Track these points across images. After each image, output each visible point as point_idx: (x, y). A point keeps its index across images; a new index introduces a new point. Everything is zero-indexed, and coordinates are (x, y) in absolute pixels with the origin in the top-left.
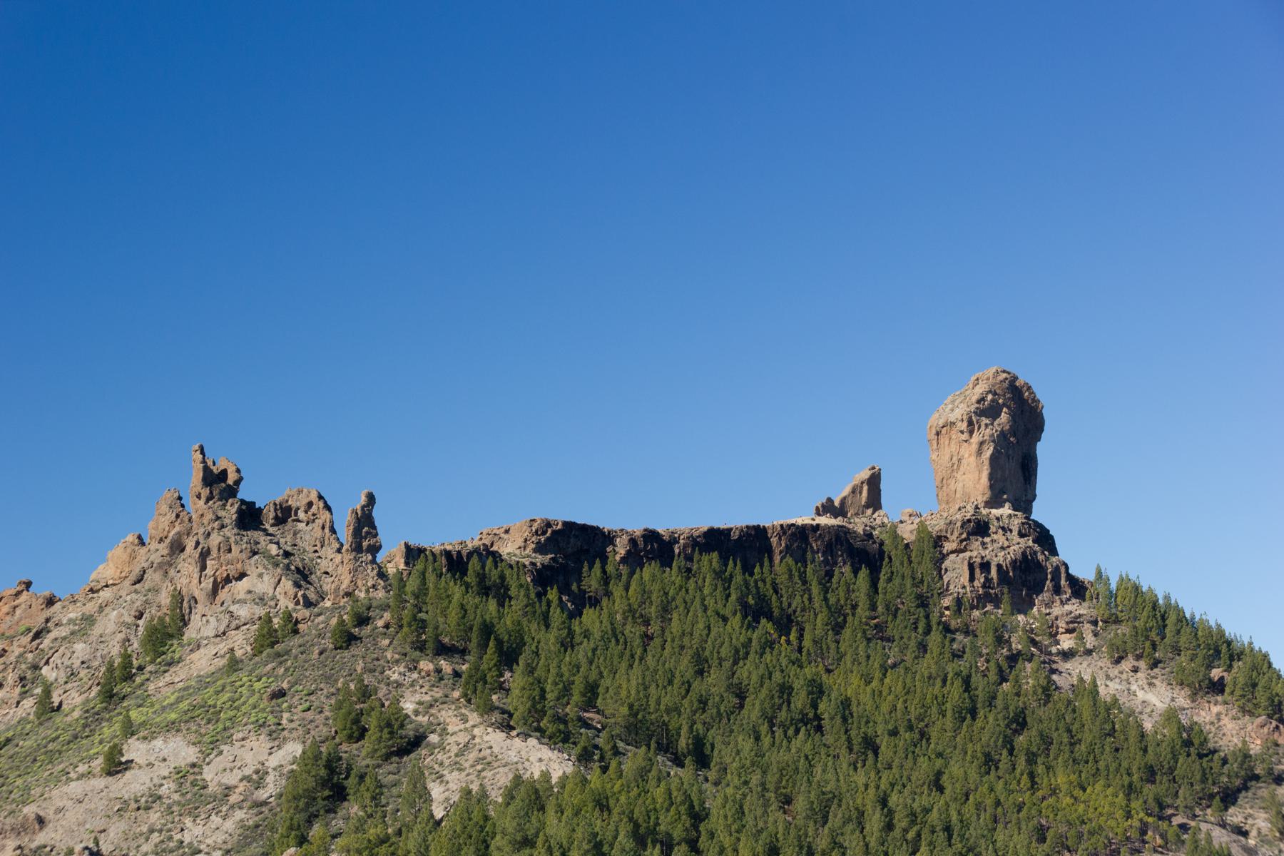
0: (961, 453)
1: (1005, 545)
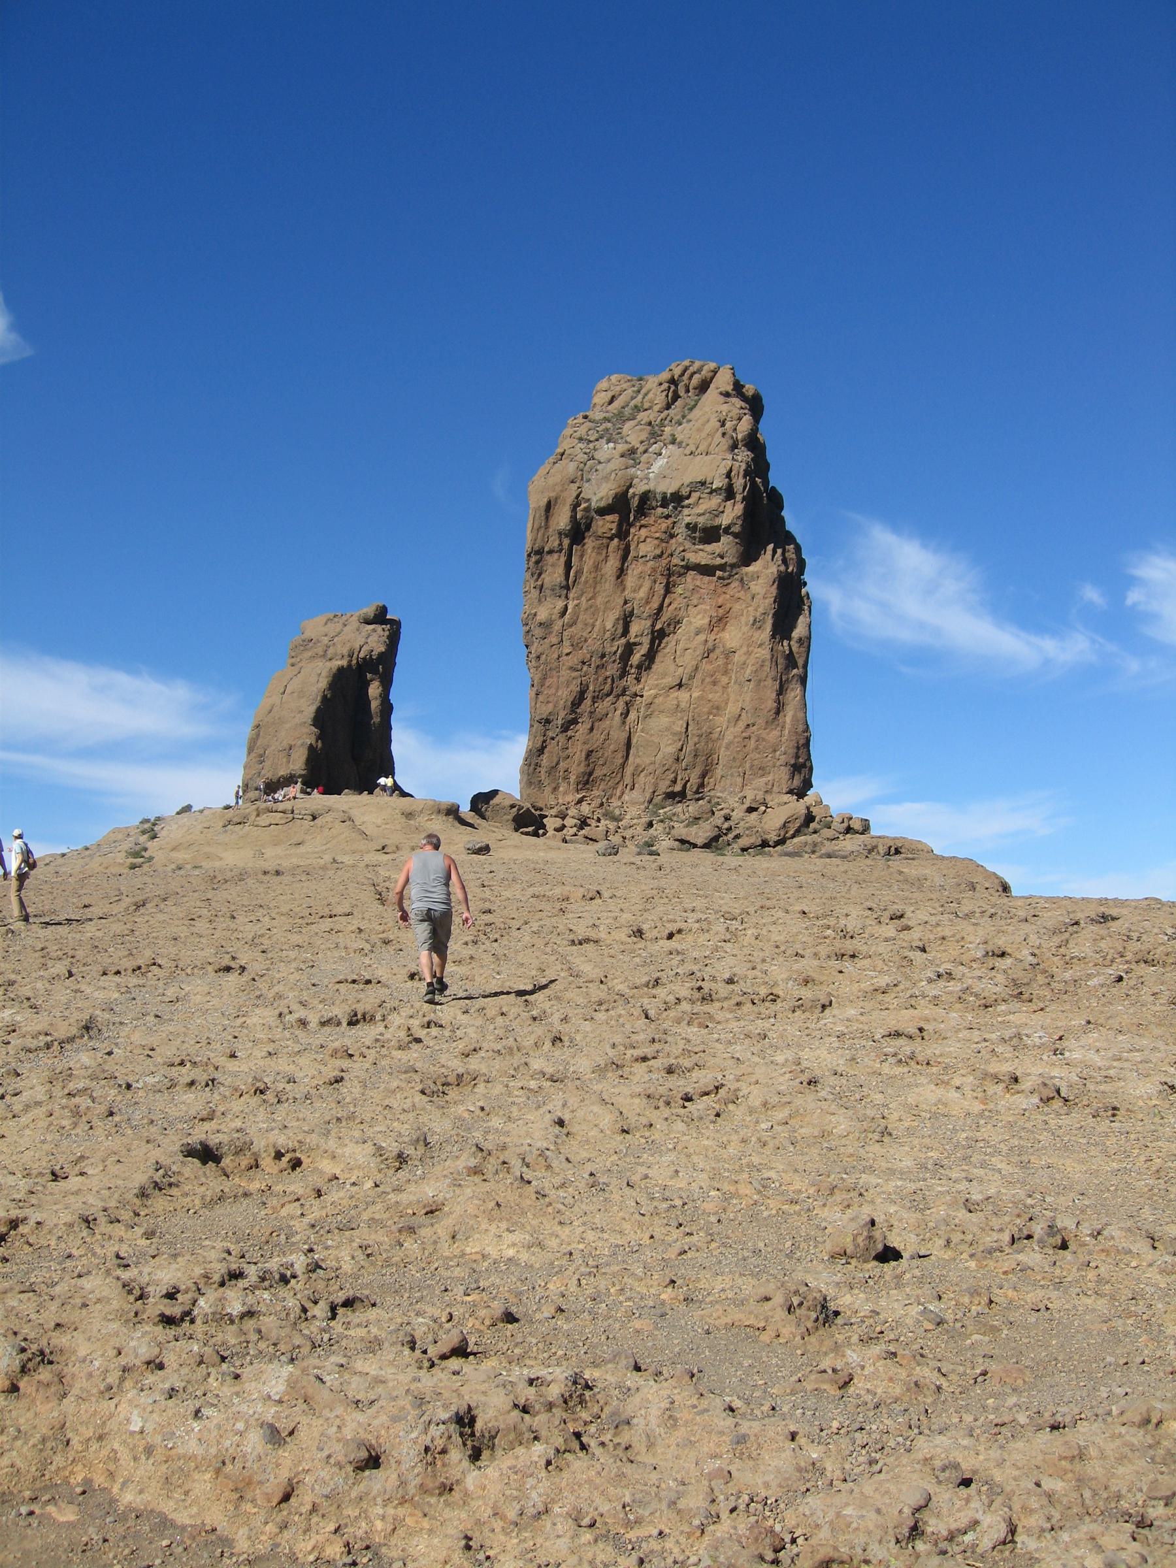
0: (666, 616)
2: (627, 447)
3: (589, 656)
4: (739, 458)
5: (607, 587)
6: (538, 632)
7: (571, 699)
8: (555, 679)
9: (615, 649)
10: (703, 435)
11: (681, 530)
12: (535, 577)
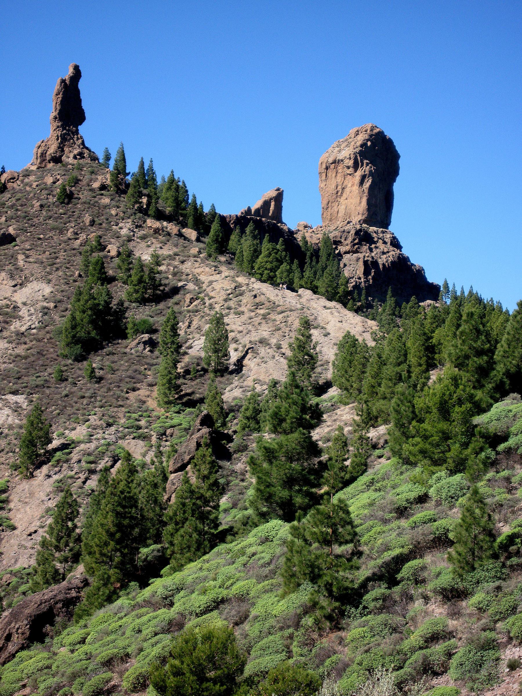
0: (344, 184)
1: (385, 251)
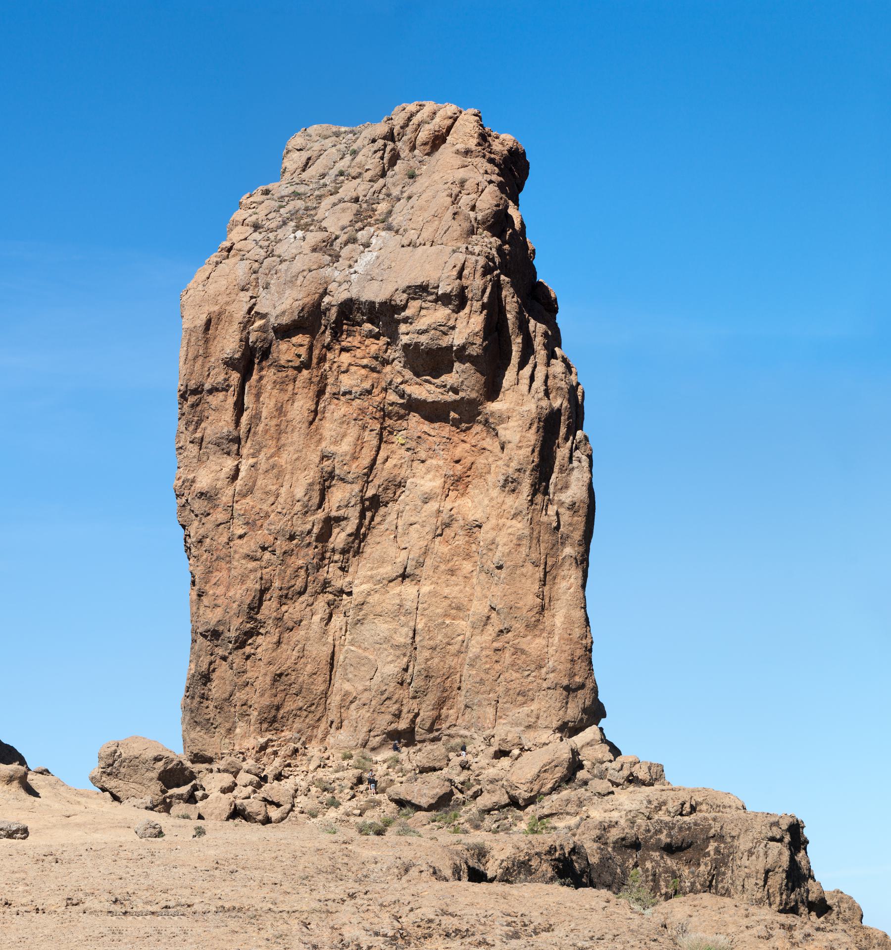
2: (324, 235)
3: (271, 538)
4: (477, 249)
5: (295, 438)
6: (199, 505)
7: (248, 602)
8: (224, 573)
9: (309, 526)
10: (427, 215)
11: (395, 353)
12: (191, 428)
